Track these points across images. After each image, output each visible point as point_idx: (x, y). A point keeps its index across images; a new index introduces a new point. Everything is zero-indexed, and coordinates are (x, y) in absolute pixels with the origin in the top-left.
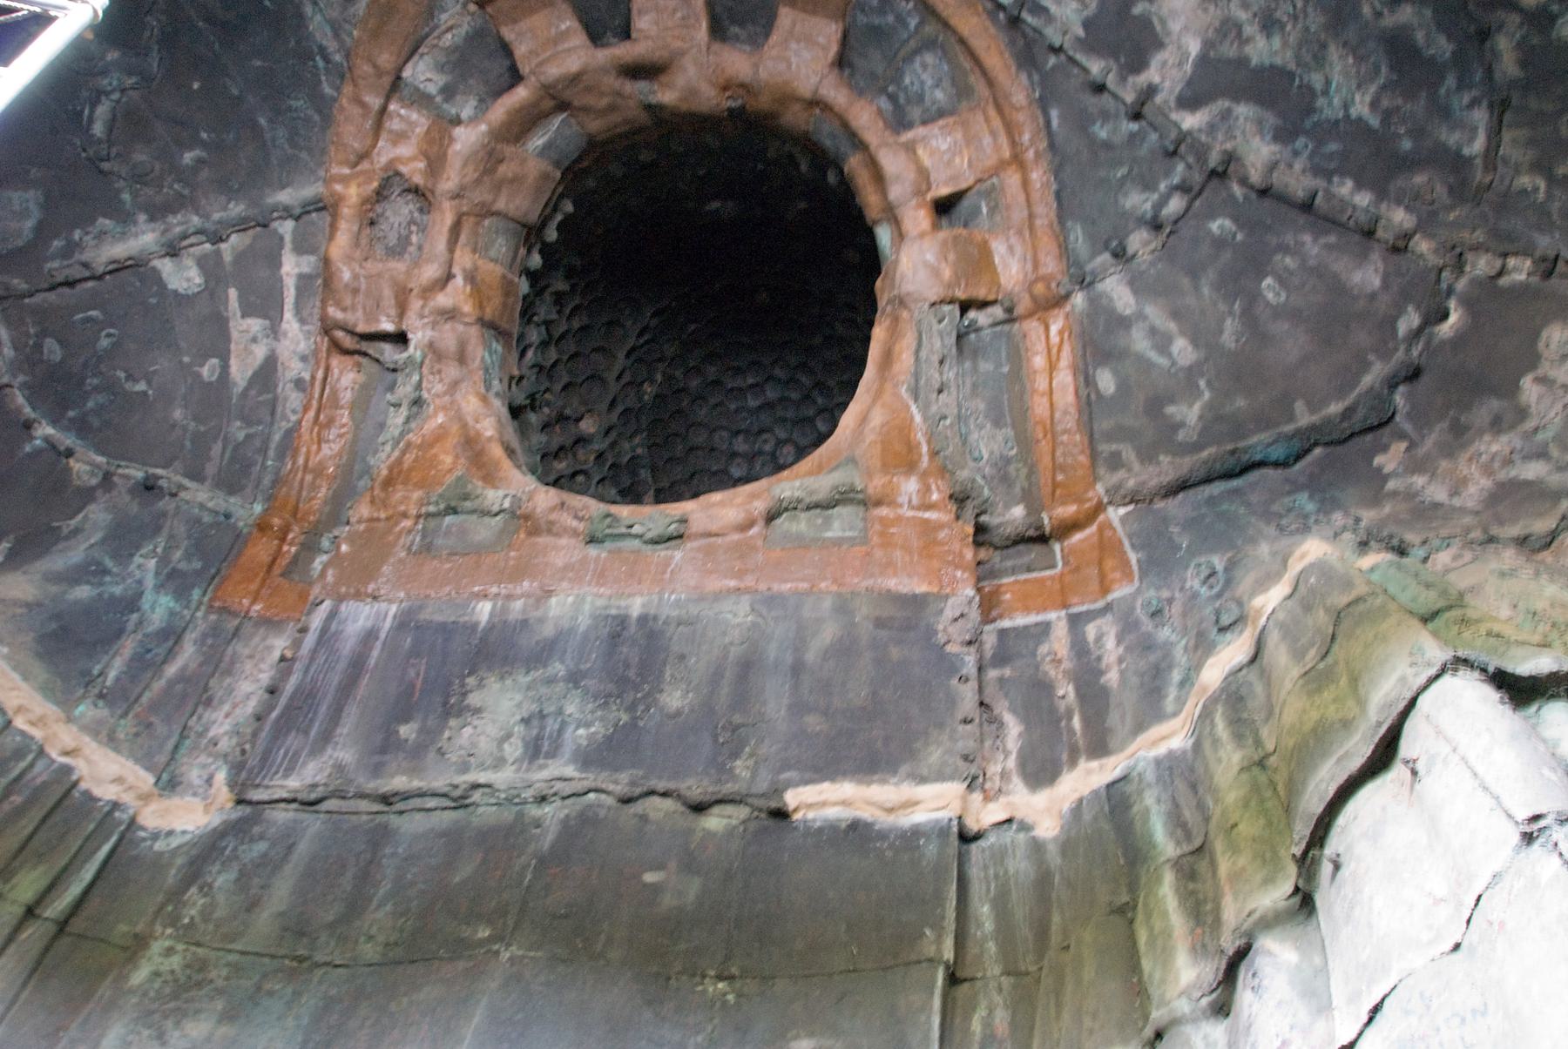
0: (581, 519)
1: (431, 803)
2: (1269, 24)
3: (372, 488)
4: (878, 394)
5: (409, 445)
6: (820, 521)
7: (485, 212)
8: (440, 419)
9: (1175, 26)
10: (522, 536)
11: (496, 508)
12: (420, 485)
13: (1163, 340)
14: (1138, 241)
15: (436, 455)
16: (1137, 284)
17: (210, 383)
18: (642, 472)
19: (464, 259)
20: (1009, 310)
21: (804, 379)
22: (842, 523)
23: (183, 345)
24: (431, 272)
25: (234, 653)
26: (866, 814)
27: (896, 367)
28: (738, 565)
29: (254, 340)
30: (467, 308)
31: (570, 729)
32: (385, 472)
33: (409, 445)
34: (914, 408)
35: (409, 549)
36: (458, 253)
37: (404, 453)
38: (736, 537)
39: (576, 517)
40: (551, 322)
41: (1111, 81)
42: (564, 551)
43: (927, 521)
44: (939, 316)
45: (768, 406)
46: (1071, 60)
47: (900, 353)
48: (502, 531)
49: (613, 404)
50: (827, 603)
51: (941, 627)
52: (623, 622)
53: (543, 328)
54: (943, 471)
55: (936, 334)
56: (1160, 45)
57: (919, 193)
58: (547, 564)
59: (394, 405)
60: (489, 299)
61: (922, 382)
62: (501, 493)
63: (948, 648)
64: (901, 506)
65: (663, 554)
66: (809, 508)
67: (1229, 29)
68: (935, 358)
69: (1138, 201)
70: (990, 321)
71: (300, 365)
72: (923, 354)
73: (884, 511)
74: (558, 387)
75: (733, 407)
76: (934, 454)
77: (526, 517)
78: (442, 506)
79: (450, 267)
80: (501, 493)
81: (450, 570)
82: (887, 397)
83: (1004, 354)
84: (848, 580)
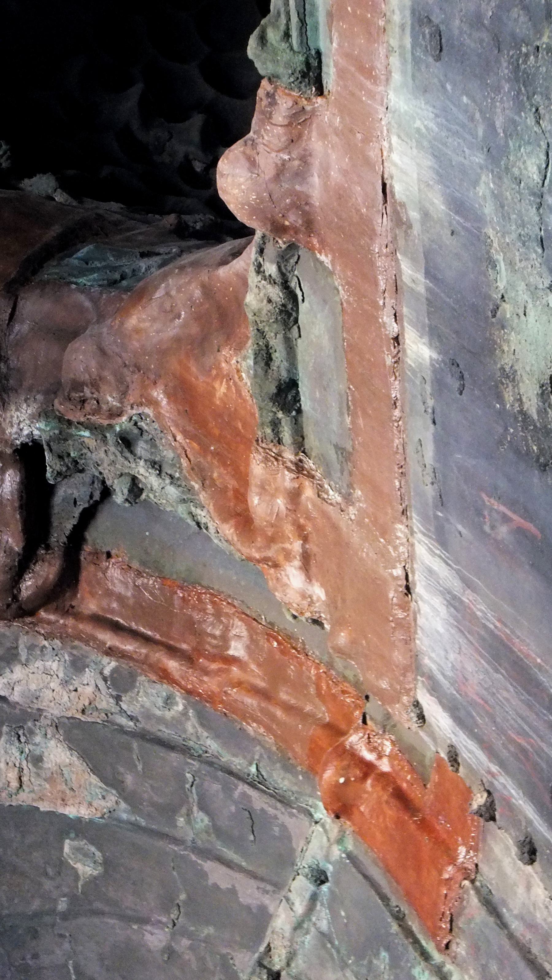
11: (276, 293)
17: (107, 863)
23: (36, 905)
25: (521, 918)
29: (37, 760)
71: (89, 676)
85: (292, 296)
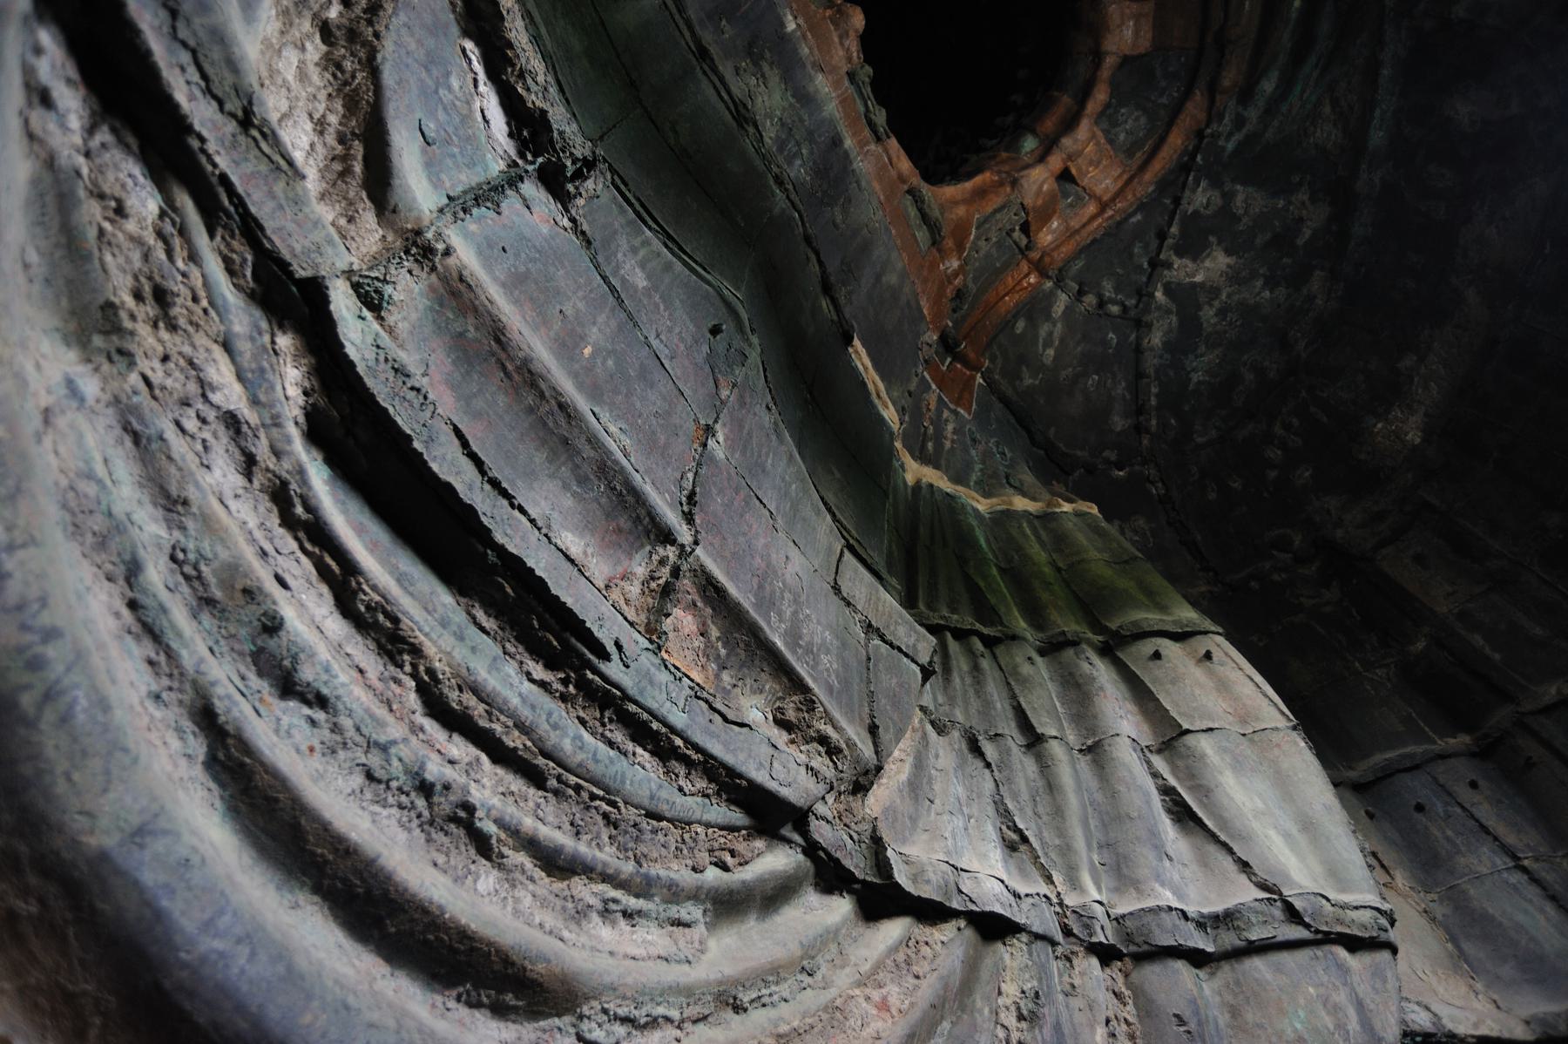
1: (726, 97)
2: (1222, 313)
9: (1207, 263)
13: (1050, 340)
14: (1090, 299)
16: (1068, 310)
20: (1028, 247)
26: (871, 387)
31: (799, 162)
41: (1170, 241)
46: (1173, 213)
56: (1194, 260)
57: (1070, 157)
67: (1214, 292)
69: (1108, 288)
72: (998, 216)
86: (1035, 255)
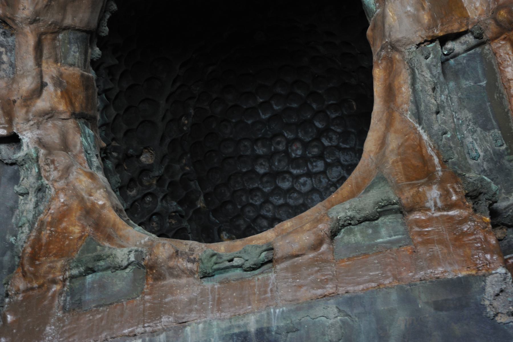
0: (193, 261)
3: (22, 265)
4: (389, 123)
5: (42, 223)
6: (370, 231)
7: (58, 28)
8: (62, 199)
10: (151, 282)
11: (125, 263)
12: (60, 254)
15: (65, 228)
18: (192, 183)
19: (50, 70)
20: (478, 37)
21: (299, 92)
22: (387, 231)
24: (27, 84)
27: (399, 100)
28: (320, 276)
30: (62, 107)
32: (29, 250)
33: (42, 223)
34: (419, 129)
35: (64, 308)
36: (44, 66)
37: (39, 231)
38: (311, 255)
39: (190, 261)
40: (110, 89)
42: (186, 289)
43: (451, 218)
44: (425, 53)
45: (276, 116)
47: (400, 88)
48: (134, 280)
49: (162, 139)
50: (394, 296)
51: (487, 303)
52: (245, 338)
53: (104, 96)
54: (455, 176)
55: (425, 69)
58: (175, 301)
59: (22, 195)
60: (76, 96)
61: (422, 108)
62: (126, 250)
63: (499, 319)
64: (429, 209)
65: (260, 277)
66: (360, 222)
68: (429, 88)
70: (465, 47)
72: (418, 86)
73: (417, 216)
74: (121, 135)
75: (249, 122)
76: (444, 163)
77: (151, 268)
78: (82, 269)
79: (42, 77)
80: (126, 250)
81: (101, 319)
82: (397, 125)
83: (480, 72)
84: (404, 275)
85: (126, 267)
86: (491, 29)
